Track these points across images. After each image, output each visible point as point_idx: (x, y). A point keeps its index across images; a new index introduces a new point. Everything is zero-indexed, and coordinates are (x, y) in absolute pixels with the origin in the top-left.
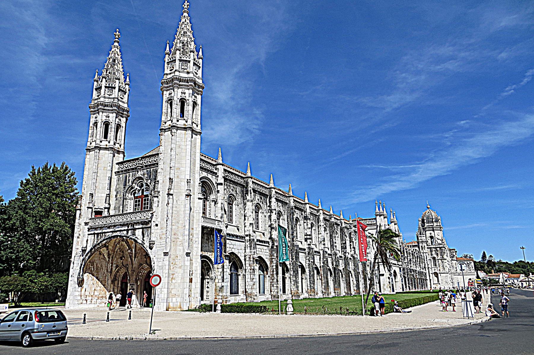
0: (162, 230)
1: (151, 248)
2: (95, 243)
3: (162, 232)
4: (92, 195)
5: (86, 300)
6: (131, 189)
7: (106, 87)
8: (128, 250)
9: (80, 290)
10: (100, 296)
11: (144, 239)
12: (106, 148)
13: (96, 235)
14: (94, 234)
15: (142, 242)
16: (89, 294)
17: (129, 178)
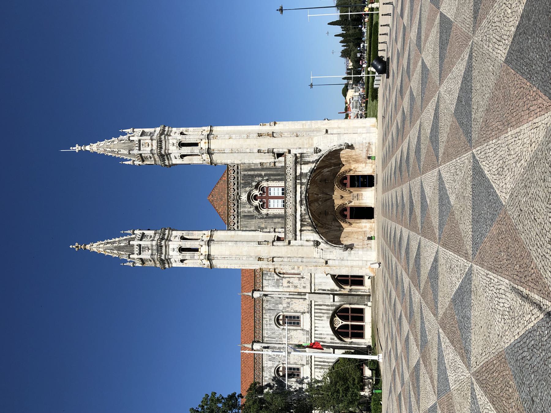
0: (305, 144)
1: (320, 151)
2: (310, 228)
3: (306, 144)
4: (259, 243)
5: (367, 244)
6: (258, 209)
7: (141, 240)
8: (319, 204)
9: (358, 249)
10: (363, 235)
11: (311, 161)
12: (211, 236)
13: (302, 229)
14: (301, 231)
15: (314, 163)
16: (361, 243)
17: (245, 212)
